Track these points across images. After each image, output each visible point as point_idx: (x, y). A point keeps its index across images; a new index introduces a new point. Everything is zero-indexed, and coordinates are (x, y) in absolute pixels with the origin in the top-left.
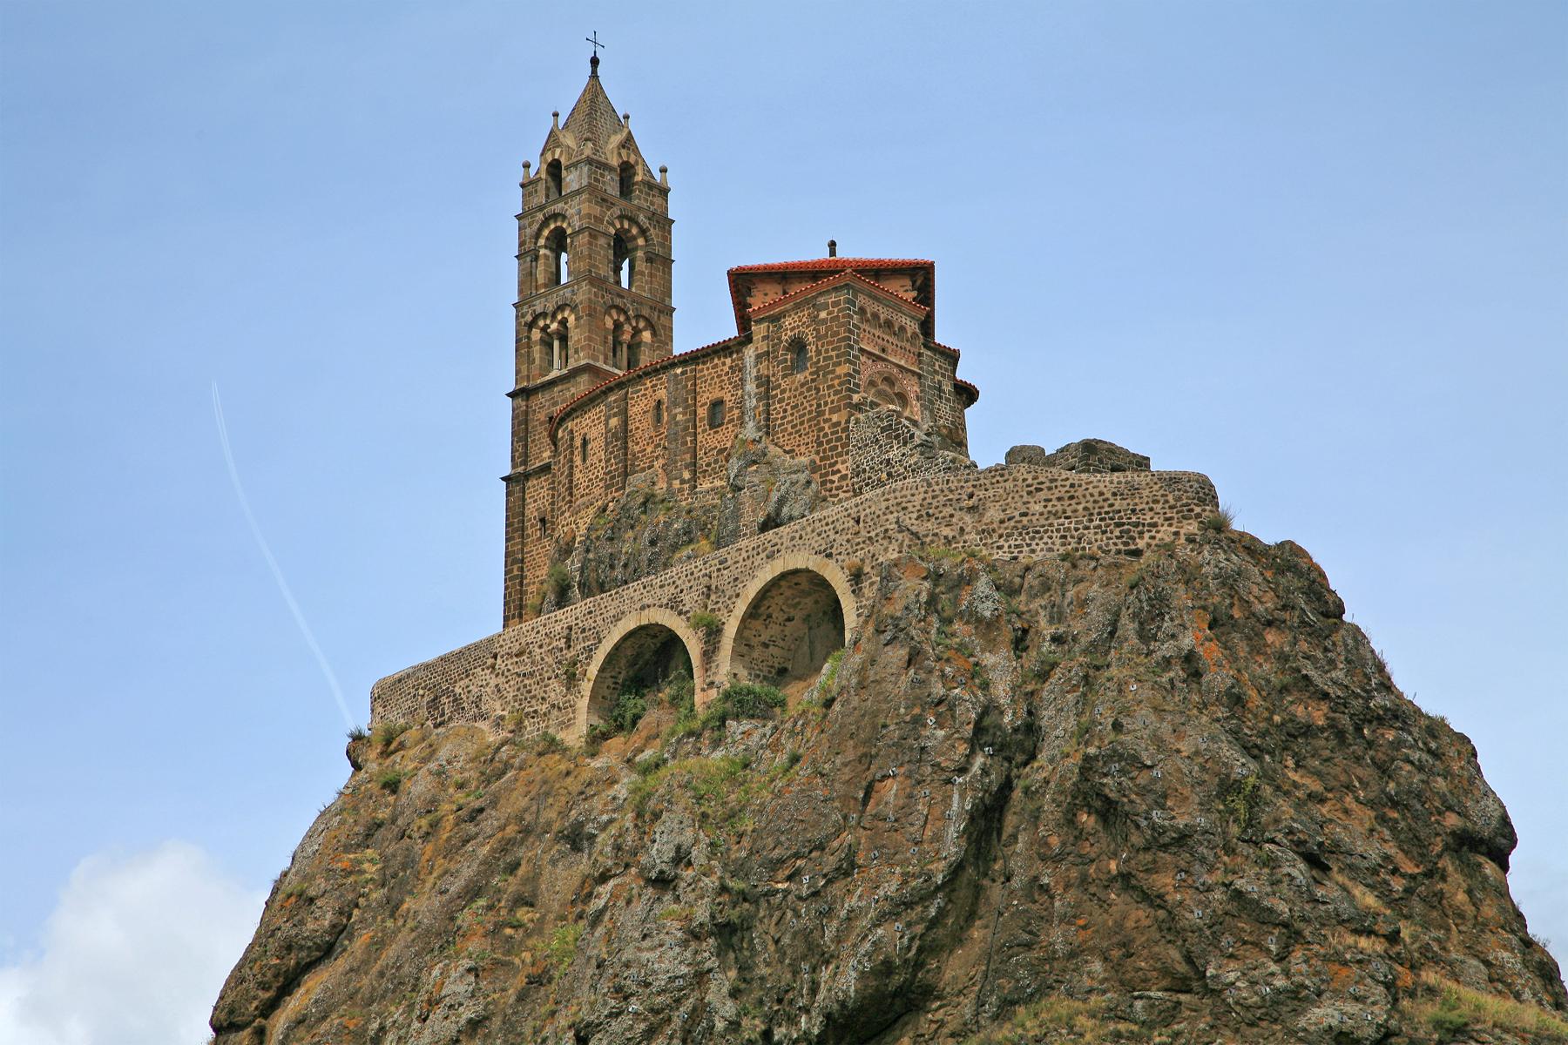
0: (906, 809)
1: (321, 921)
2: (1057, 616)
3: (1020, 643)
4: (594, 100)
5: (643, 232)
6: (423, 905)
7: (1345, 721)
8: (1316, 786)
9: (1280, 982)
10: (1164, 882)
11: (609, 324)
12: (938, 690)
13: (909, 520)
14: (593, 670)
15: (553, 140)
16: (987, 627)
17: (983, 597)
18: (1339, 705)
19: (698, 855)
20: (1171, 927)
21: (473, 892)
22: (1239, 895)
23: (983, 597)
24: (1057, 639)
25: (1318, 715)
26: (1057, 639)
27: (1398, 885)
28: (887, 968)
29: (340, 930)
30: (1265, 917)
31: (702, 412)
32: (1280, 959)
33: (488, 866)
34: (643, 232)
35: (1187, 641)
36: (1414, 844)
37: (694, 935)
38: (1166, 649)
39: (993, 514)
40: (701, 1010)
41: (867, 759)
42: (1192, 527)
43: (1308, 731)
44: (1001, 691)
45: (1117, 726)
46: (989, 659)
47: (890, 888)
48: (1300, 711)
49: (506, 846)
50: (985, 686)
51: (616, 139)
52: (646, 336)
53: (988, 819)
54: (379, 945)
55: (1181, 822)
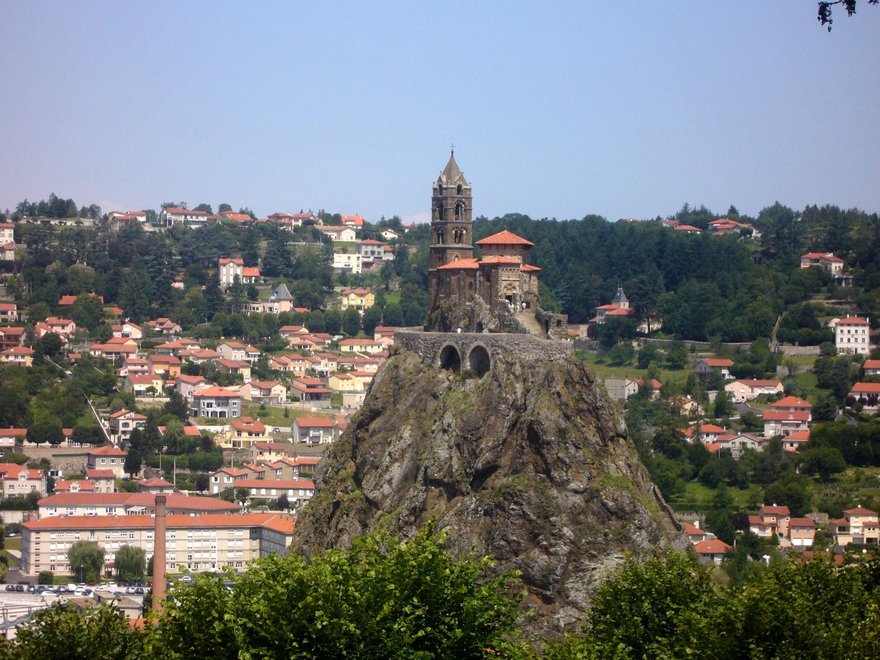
0: (495, 424)
1: (379, 404)
2: (533, 376)
3: (525, 380)
4: (451, 169)
5: (464, 203)
6: (401, 407)
7: (591, 408)
8: (583, 423)
9: (565, 478)
10: (545, 451)
11: (454, 232)
12: (504, 395)
13: (503, 344)
14: (440, 351)
15: (440, 179)
16: (516, 377)
17: (518, 370)
18: (589, 405)
19: (453, 425)
20: (545, 461)
21: (412, 406)
22: (558, 457)
23: (518, 370)
24: (532, 382)
25: (585, 407)
26: (532, 382)
27: (598, 448)
28: (489, 462)
29: (384, 408)
30: (564, 462)
31: (467, 284)
32: (566, 472)
33: (415, 400)
34: (464, 203)
35: (558, 389)
36: (603, 439)
37: (450, 448)
38: (553, 390)
39: (522, 346)
40: (451, 466)
41: (487, 409)
42: (564, 355)
43: (583, 411)
44: (519, 394)
45: (538, 413)
46: (517, 385)
47: (490, 444)
48: (581, 406)
49: (420, 395)
50: (515, 393)
51: (457, 178)
52: (464, 232)
53: (513, 426)
54: (391, 416)
55: (549, 439)
